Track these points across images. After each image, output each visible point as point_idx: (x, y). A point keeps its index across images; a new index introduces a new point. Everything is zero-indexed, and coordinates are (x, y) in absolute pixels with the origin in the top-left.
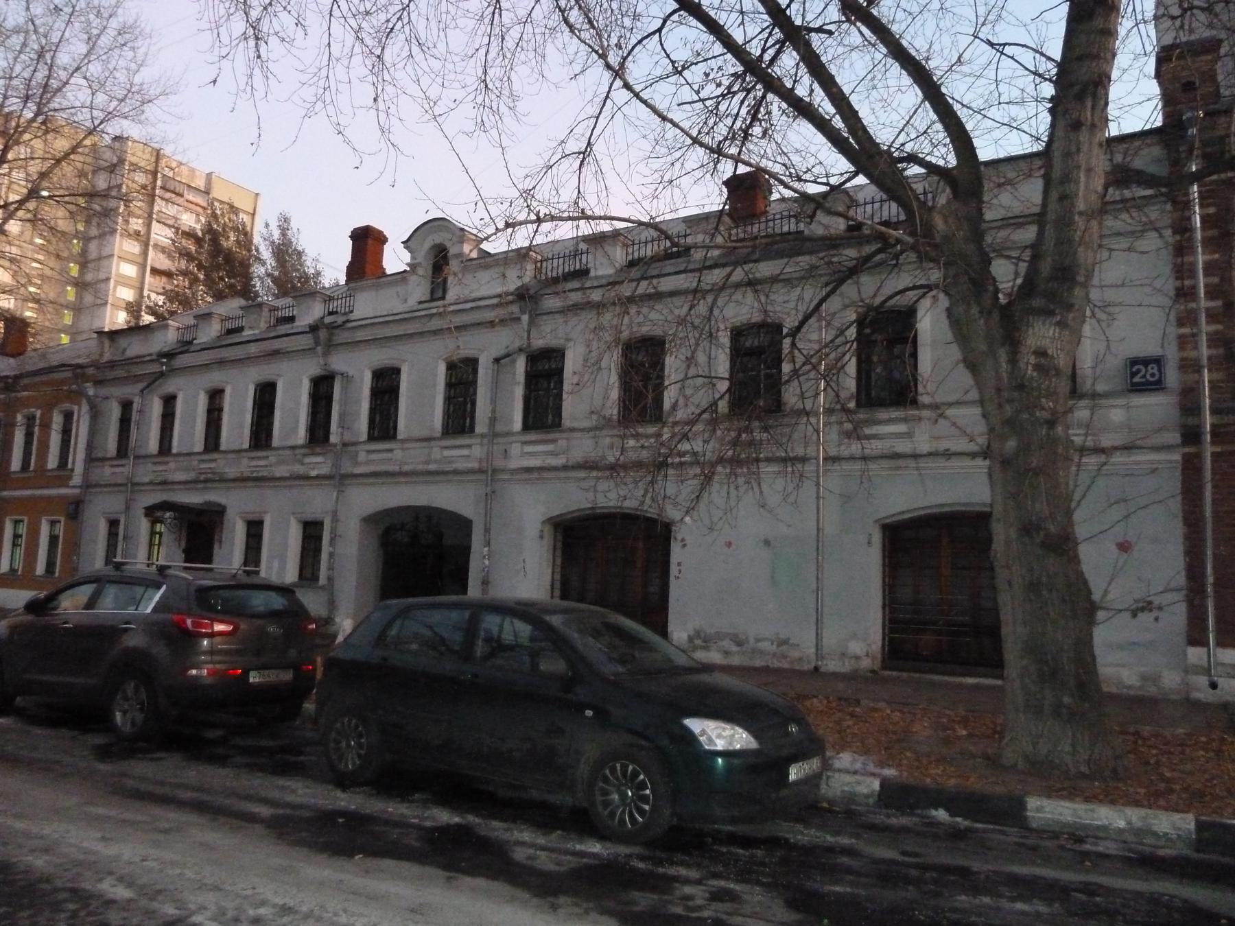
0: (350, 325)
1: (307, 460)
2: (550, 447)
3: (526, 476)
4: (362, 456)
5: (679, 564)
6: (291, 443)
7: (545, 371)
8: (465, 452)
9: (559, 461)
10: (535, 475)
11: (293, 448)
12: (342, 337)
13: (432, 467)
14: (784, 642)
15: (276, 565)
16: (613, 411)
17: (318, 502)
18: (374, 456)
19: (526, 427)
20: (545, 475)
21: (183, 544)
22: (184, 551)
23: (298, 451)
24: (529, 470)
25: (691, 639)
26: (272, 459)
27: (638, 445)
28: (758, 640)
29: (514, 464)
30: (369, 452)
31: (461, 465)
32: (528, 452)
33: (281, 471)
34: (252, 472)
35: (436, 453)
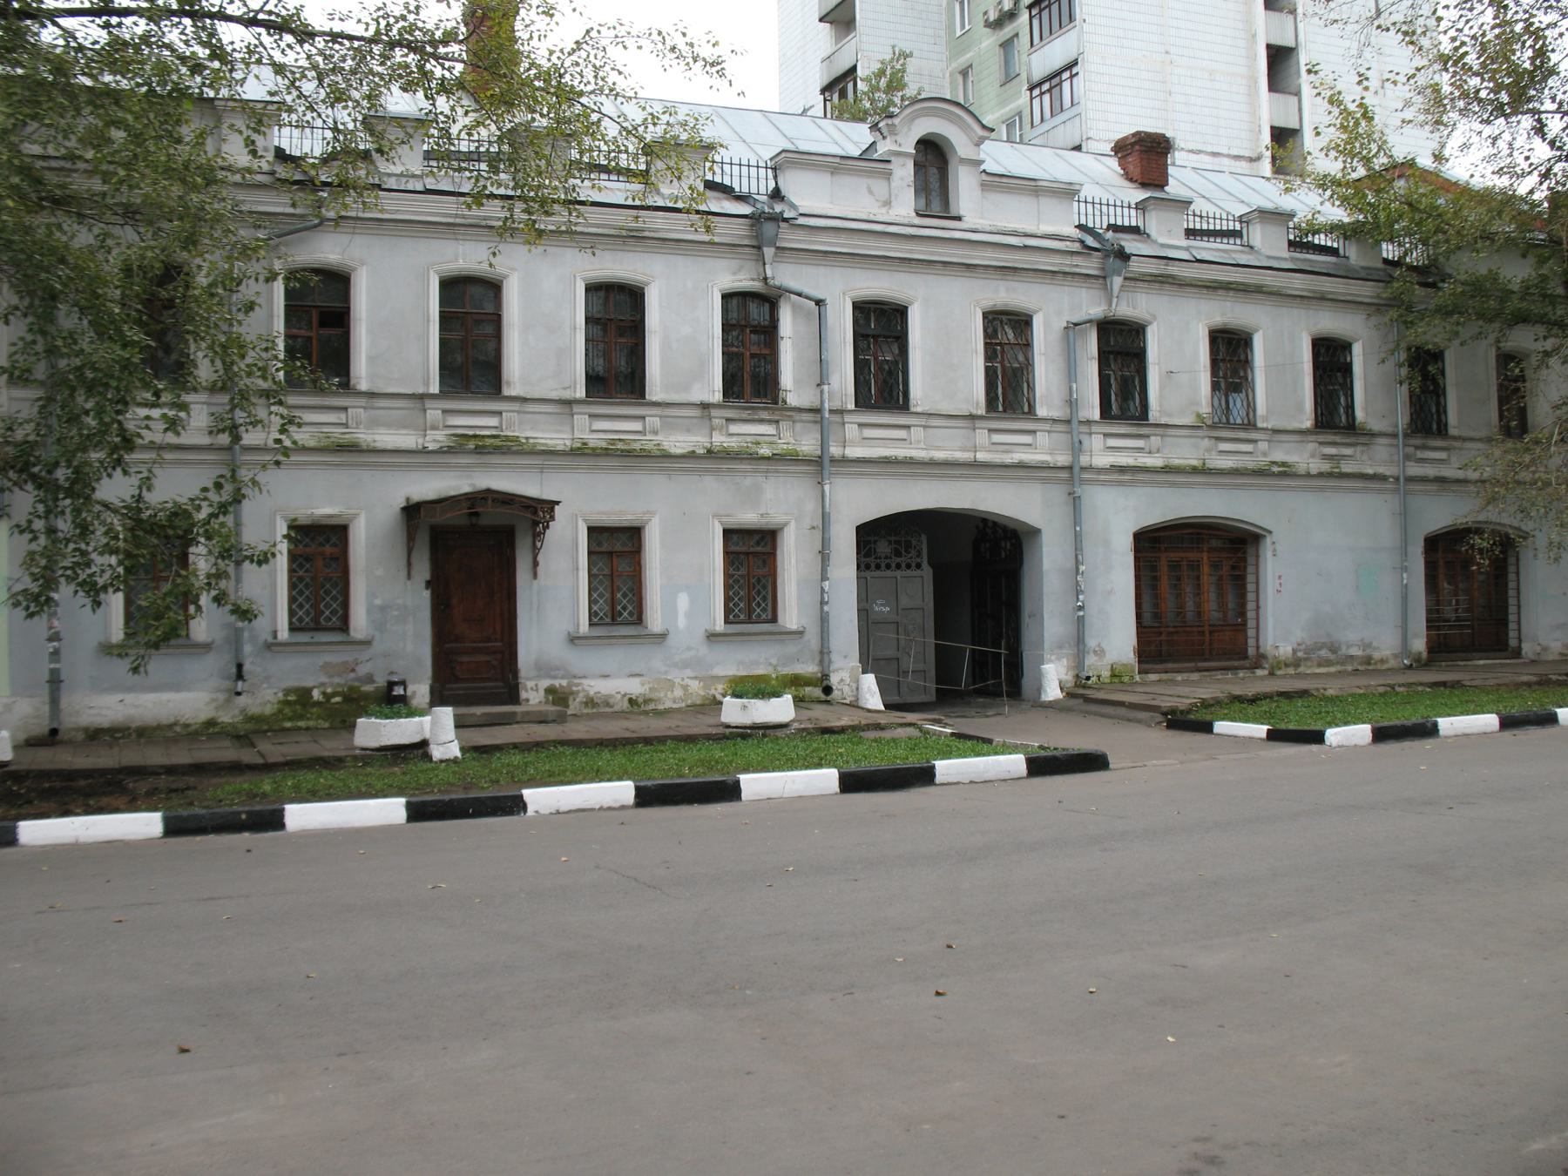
1: (734, 428)
2: (1140, 443)
4: (851, 431)
6: (698, 395)
7: (1122, 347)
11: (705, 406)
14: (1366, 646)
15: (683, 601)
18: (868, 433)
20: (1141, 477)
21: (423, 570)
22: (428, 584)
23: (714, 412)
24: (1122, 469)
26: (653, 421)
30: (861, 425)
33: (678, 442)
35: (981, 436)
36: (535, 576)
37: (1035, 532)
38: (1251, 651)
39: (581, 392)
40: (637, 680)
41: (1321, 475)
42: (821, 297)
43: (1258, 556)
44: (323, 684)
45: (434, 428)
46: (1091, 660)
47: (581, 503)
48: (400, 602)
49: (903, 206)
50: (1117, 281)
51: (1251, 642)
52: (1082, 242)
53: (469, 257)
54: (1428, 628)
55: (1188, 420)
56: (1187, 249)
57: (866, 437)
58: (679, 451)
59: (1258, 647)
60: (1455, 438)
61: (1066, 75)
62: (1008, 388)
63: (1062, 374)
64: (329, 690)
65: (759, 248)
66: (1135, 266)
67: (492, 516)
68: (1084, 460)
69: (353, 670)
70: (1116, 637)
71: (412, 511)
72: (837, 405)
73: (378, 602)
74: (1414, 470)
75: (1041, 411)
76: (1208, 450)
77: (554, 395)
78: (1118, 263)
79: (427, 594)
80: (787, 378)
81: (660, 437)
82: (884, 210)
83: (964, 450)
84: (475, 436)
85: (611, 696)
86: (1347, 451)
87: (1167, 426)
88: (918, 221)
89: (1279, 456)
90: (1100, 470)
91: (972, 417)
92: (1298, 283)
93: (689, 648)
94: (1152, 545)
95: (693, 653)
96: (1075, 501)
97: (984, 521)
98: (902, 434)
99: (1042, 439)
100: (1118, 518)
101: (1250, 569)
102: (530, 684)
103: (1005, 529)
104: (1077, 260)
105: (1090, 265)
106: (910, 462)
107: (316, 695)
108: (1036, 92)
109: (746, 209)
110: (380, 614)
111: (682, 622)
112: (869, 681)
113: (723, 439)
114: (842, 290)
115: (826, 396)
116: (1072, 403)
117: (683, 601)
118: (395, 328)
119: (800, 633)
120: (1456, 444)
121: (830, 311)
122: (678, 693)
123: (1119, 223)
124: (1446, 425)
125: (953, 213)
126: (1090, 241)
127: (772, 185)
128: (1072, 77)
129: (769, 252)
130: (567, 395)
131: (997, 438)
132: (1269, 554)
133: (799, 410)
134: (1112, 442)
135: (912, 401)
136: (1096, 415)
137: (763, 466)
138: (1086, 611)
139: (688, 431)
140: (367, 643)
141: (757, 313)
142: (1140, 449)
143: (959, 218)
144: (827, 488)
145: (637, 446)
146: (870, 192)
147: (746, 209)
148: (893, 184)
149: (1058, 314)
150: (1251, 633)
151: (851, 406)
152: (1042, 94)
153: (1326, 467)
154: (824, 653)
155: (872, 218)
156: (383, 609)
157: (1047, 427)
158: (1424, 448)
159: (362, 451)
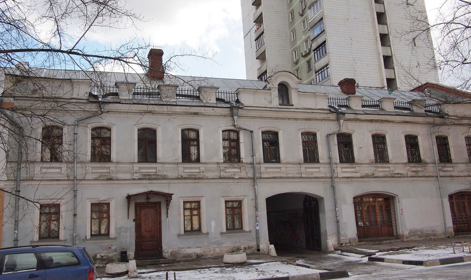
0: (245, 108)
1: (227, 170)
2: (353, 170)
3: (346, 180)
5: (402, 210)
6: (216, 160)
8: (317, 170)
9: (358, 175)
10: (350, 180)
11: (218, 163)
12: (241, 112)
13: (303, 176)
15: (213, 223)
16: (373, 158)
17: (239, 191)
18: (268, 170)
19: (340, 162)
20: (354, 179)
21: (132, 216)
24: (348, 178)
25: (409, 234)
27: (381, 170)
28: (427, 231)
29: (341, 175)
30: (265, 168)
31: (317, 175)
32: (343, 170)
34: (190, 175)
35: (303, 170)
36: (167, 217)
37: (322, 199)
38: (395, 234)
39: (180, 160)
40: (200, 248)
41: (412, 177)
42: (252, 129)
43: (394, 203)
44: (101, 253)
45: (136, 173)
46: (342, 238)
47: (180, 193)
48: (125, 226)
49: (276, 102)
50: (342, 121)
51: (394, 231)
52: (330, 110)
53: (148, 122)
54: (453, 224)
55: (367, 161)
56: (363, 110)
57: (269, 169)
58: (210, 177)
59: (397, 232)
60: (455, 163)
61: (326, 68)
62: (310, 155)
63: (327, 150)
64: (103, 255)
65: (233, 116)
66: (347, 116)
67: (154, 199)
68: (335, 175)
69: (110, 248)
70: (350, 230)
71: (129, 198)
72: (258, 161)
73: (118, 226)
74: (442, 174)
75: (321, 161)
76: (375, 171)
77: (172, 162)
78: (341, 116)
79: (134, 223)
80: (243, 155)
81: (204, 174)
82: (270, 104)
83: (298, 173)
84: (149, 175)
85: (191, 254)
86: (420, 169)
87: (361, 164)
88: (280, 107)
89: (397, 171)
90: (340, 178)
91: (300, 164)
92: (398, 118)
93: (215, 238)
94: (358, 201)
95: (216, 239)
96: (333, 187)
97: (306, 195)
98: (279, 170)
99: (322, 169)
100: (348, 193)
101: (392, 207)
102: (166, 251)
103: (313, 198)
104: (329, 116)
105: (333, 116)
106: (281, 178)
107: (98, 256)
108: (317, 74)
109: (229, 106)
110: (119, 230)
111: (213, 230)
112: (272, 246)
113: (224, 173)
114: (258, 127)
115: (254, 159)
116: (330, 158)
117: (213, 223)
118: (124, 145)
119: (250, 231)
120: (455, 165)
121: (255, 134)
122: (212, 252)
123: (341, 104)
124: (451, 159)
125: (291, 104)
126: (332, 110)
127: (236, 98)
128: (327, 68)
129: (235, 118)
130: (177, 161)
131: (308, 170)
132: (397, 202)
133: (247, 164)
134: (344, 170)
135: (281, 160)
136: (338, 161)
137: (236, 181)
138: (340, 221)
139: (213, 171)
140: (115, 239)
141: (233, 136)
142: (353, 172)
143: (292, 105)
144: (256, 187)
145: (197, 177)
146: (265, 99)
147: (229, 106)
148: (272, 97)
149: (324, 130)
150: (394, 228)
151: (262, 161)
152: (319, 74)
153: (413, 174)
154: (258, 238)
155: (266, 106)
156: (120, 228)
157: (323, 166)
158: (445, 167)
159: (114, 180)
